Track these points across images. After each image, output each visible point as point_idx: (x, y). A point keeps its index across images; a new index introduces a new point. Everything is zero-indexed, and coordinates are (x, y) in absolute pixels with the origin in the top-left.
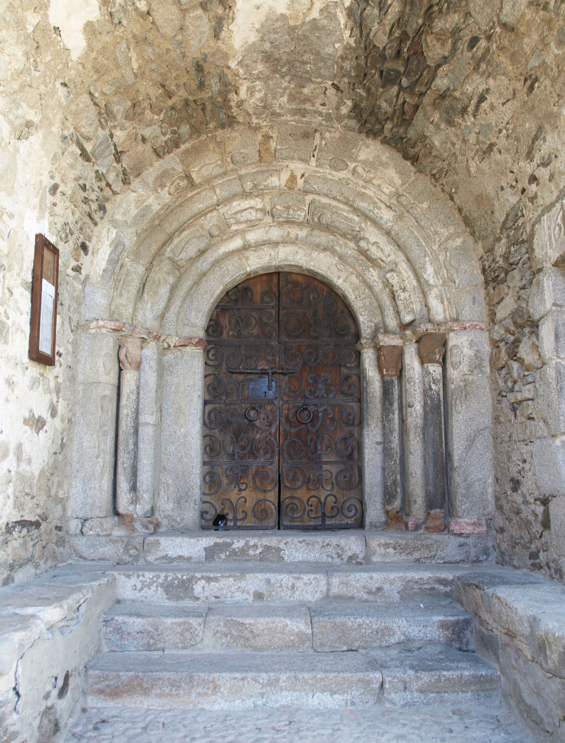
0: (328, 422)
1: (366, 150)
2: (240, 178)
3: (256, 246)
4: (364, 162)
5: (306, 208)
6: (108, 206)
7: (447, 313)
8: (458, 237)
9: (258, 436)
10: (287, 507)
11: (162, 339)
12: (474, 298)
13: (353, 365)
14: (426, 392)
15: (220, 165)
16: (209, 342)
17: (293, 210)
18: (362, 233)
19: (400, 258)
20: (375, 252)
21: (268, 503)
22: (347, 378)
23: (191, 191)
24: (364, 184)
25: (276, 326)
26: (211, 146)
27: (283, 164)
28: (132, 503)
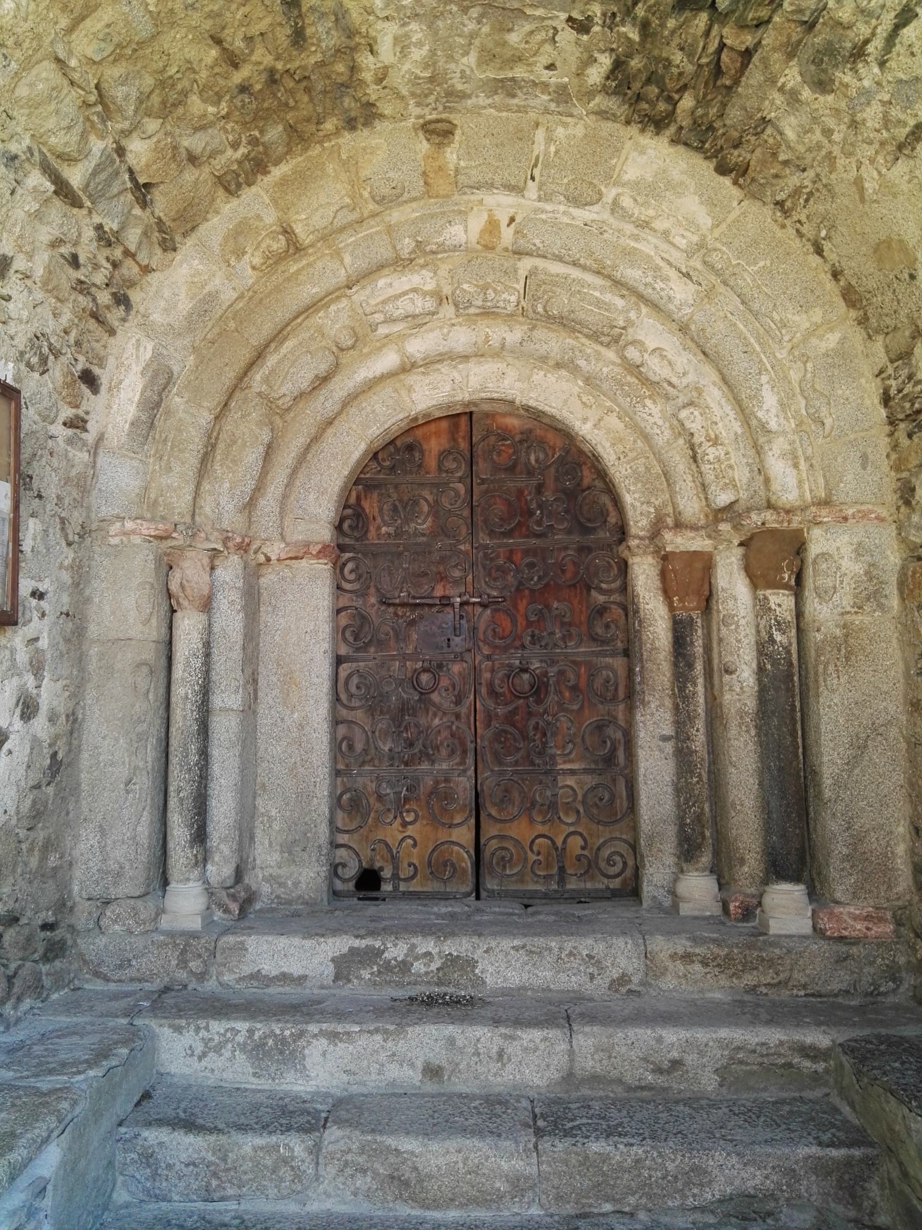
0: (567, 694)
1: (639, 159)
2: (390, 229)
4: (636, 185)
5: (520, 286)
6: (135, 296)
7: (806, 486)
8: (832, 330)
9: (437, 721)
10: (493, 854)
11: (254, 547)
12: (864, 458)
13: (613, 586)
14: (763, 647)
15: (348, 206)
16: (342, 548)
17: (495, 290)
18: (630, 330)
19: (709, 377)
20: (656, 368)
21: (456, 848)
23: (295, 261)
24: (636, 231)
25: (466, 513)
26: (330, 168)
27: (472, 198)
28: (196, 864)
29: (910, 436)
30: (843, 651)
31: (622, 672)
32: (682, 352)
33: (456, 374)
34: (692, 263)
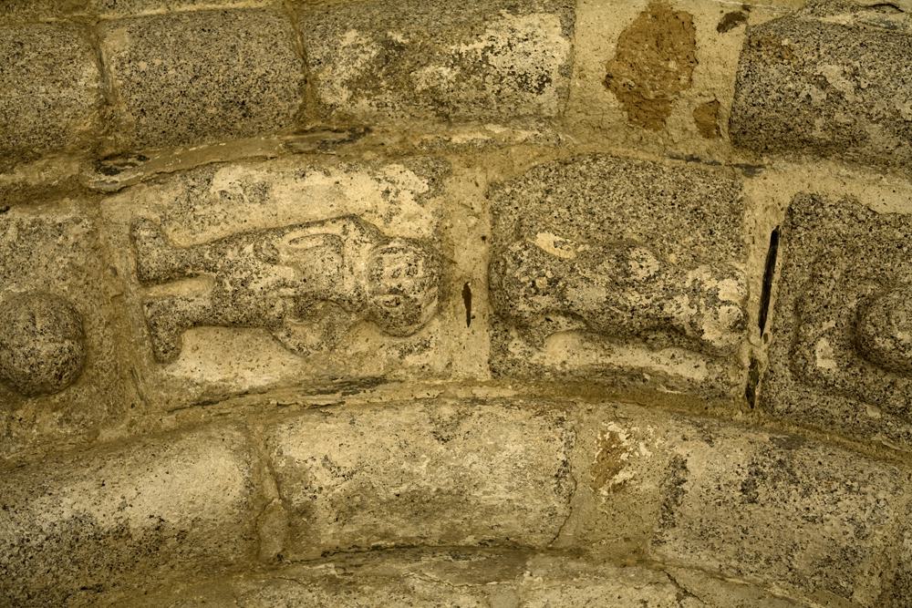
3: (350, 555)
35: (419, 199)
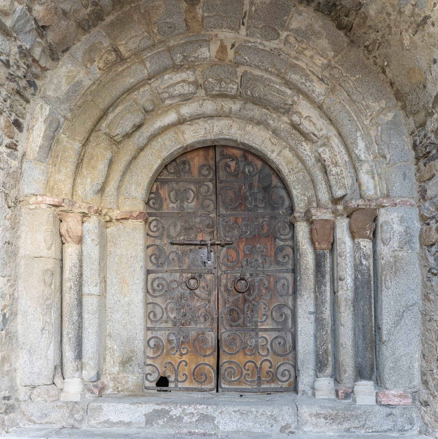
0: (264, 291)
6: (39, 83)
7: (378, 188)
14: (357, 268)
19: (332, 133)
20: (307, 126)
22: (282, 249)
29: (425, 165)
30: (394, 269)
31: (291, 280)
32: (320, 118)
33: (207, 125)
34: (324, 73)
35: (192, 75)
